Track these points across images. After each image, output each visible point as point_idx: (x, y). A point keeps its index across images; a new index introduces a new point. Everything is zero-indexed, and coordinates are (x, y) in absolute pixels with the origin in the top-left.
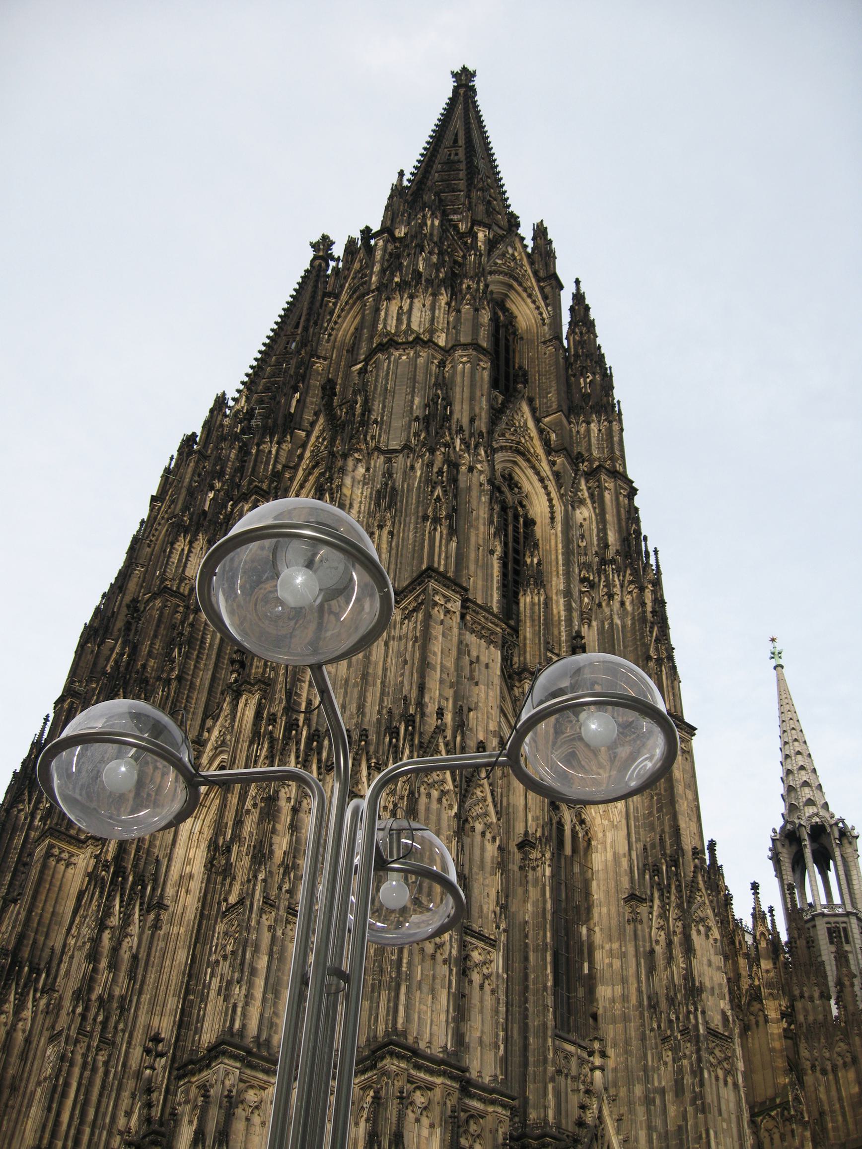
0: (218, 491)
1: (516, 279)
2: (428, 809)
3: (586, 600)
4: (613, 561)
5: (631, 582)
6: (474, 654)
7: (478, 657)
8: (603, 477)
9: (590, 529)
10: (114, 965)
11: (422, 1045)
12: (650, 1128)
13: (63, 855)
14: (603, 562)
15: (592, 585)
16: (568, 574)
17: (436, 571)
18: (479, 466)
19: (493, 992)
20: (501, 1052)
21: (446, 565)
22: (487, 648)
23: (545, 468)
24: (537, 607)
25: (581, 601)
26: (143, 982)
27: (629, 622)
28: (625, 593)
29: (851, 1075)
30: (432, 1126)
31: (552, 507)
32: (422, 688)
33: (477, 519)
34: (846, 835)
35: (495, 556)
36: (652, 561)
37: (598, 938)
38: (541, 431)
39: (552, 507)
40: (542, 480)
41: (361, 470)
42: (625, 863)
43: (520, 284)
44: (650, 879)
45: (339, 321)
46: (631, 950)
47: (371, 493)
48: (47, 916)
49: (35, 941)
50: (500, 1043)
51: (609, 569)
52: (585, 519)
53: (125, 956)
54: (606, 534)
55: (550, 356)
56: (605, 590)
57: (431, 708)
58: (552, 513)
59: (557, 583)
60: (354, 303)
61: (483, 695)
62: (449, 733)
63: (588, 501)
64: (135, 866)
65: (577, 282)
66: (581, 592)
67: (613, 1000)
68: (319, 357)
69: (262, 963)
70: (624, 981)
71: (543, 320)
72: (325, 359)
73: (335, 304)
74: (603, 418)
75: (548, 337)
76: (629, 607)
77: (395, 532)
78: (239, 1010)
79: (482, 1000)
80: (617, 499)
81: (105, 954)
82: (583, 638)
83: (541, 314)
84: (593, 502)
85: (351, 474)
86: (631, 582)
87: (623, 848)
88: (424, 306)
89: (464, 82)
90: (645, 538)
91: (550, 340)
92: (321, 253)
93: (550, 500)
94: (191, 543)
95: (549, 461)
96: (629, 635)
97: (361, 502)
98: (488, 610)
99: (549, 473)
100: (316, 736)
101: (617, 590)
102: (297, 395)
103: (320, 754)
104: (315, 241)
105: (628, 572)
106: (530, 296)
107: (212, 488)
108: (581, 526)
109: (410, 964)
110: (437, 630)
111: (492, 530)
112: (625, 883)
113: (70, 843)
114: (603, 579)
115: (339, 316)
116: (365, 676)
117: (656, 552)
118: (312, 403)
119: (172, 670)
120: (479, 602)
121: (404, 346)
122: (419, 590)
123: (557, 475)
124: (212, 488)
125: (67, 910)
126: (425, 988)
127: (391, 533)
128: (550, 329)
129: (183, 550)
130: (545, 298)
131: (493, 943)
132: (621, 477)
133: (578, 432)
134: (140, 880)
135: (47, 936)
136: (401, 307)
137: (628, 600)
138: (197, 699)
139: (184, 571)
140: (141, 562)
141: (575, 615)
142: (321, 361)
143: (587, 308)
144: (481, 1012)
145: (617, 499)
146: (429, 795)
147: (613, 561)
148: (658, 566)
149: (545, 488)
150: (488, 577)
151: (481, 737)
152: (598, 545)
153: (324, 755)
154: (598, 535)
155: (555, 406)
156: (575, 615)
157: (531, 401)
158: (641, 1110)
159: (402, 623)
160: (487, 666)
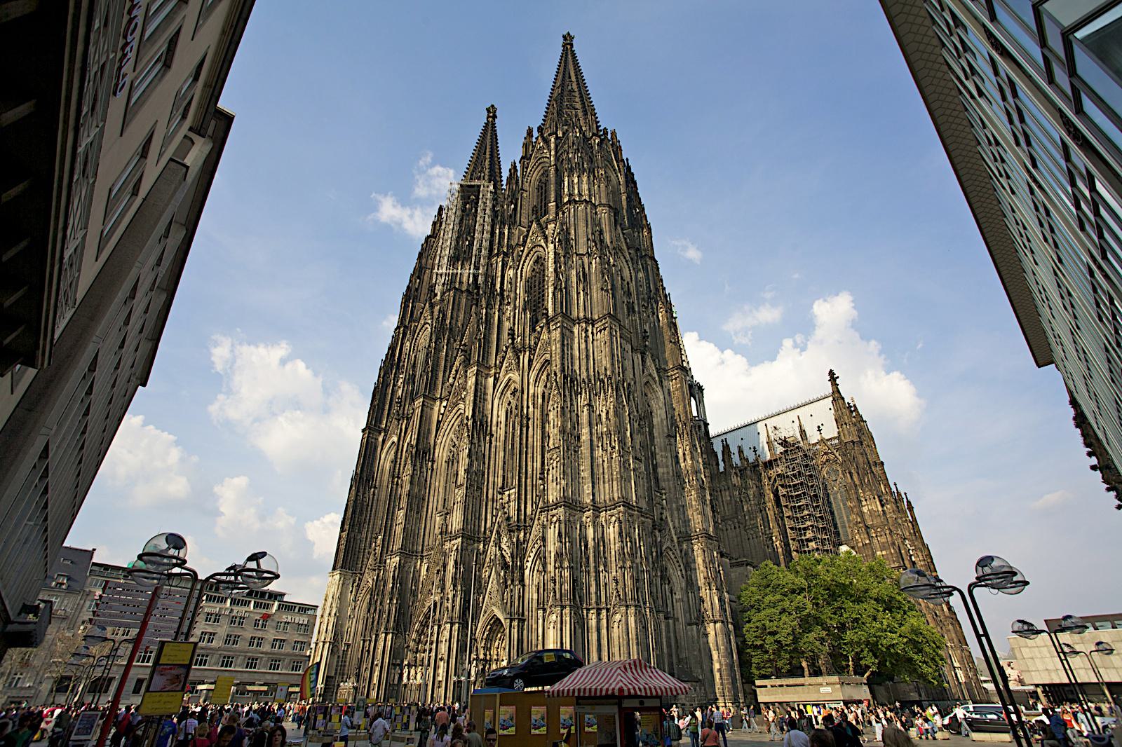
12: (679, 519)
14: (649, 298)
15: (646, 308)
16: (638, 304)
29: (727, 493)
34: (701, 389)
37: (657, 451)
40: (627, 261)
46: (669, 455)
67: (663, 473)
70: (667, 467)
131: (641, 461)
143: (633, 174)
158: (675, 512)
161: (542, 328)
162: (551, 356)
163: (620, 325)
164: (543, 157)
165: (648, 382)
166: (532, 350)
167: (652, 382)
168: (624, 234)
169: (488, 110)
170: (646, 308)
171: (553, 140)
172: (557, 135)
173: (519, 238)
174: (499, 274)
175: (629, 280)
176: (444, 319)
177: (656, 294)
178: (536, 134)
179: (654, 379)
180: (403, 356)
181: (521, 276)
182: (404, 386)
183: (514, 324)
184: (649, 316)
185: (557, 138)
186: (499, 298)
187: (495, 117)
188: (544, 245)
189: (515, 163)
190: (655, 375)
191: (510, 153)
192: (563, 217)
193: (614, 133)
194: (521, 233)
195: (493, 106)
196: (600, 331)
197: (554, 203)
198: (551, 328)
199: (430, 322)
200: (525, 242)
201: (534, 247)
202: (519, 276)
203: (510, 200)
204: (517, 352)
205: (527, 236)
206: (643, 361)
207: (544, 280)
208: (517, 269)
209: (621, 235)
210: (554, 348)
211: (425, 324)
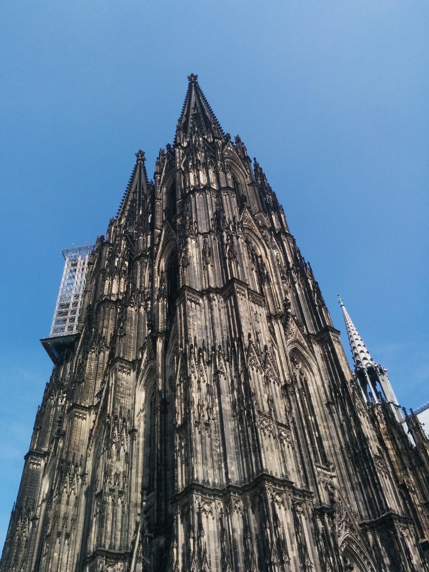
0: (120, 258)
2: (253, 375)
3: (285, 285)
6: (255, 310)
7: (256, 312)
10: (118, 459)
11: (274, 475)
13: (81, 415)
14: (289, 269)
17: (235, 279)
18: (240, 236)
19: (293, 448)
20: (302, 473)
21: (238, 276)
22: (259, 308)
25: (283, 286)
26: (132, 464)
30: (285, 509)
32: (240, 326)
33: (244, 257)
35: (254, 271)
38: (255, 220)
40: (259, 239)
41: (194, 242)
42: (322, 389)
43: (235, 162)
44: (335, 393)
47: (200, 251)
48: (77, 442)
49: (74, 454)
50: (301, 470)
53: (122, 453)
55: (252, 190)
57: (245, 334)
59: (274, 279)
60: (169, 176)
61: (261, 327)
62: (254, 343)
64: (121, 414)
65: (255, 159)
66: (283, 282)
68: (158, 199)
69: (199, 448)
72: (161, 200)
73: (160, 177)
75: (249, 182)
78: (195, 469)
79: (289, 453)
80: (289, 244)
81: (115, 454)
82: (288, 300)
85: (190, 244)
87: (320, 383)
88: (204, 173)
90: (303, 258)
91: (251, 183)
93: (264, 247)
94: (112, 280)
97: (196, 255)
98: (256, 292)
100: (200, 351)
103: (203, 358)
106: (240, 166)
107: (117, 256)
109: (262, 440)
110: (240, 303)
112: (324, 397)
113: (83, 410)
116: (213, 324)
117: (309, 263)
118: (159, 218)
119: (122, 332)
120: (252, 289)
122: (230, 287)
123: (264, 237)
124: (117, 256)
125: (85, 438)
126: (270, 450)
127: (212, 266)
129: (109, 283)
130: (245, 166)
131: (288, 427)
134: (124, 421)
135: (78, 450)
136: (195, 175)
139: (111, 291)
140: (88, 290)
141: (283, 291)
142: (159, 200)
144: (290, 457)
145: (289, 244)
146: (253, 369)
147: (293, 269)
150: (253, 280)
151: (265, 344)
156: (283, 291)
157: (249, 208)
160: (260, 315)
163: (248, 289)
171: (178, 150)
175: (264, 255)
179: (302, 345)
190: (304, 341)
201: (168, 242)
206: (285, 326)
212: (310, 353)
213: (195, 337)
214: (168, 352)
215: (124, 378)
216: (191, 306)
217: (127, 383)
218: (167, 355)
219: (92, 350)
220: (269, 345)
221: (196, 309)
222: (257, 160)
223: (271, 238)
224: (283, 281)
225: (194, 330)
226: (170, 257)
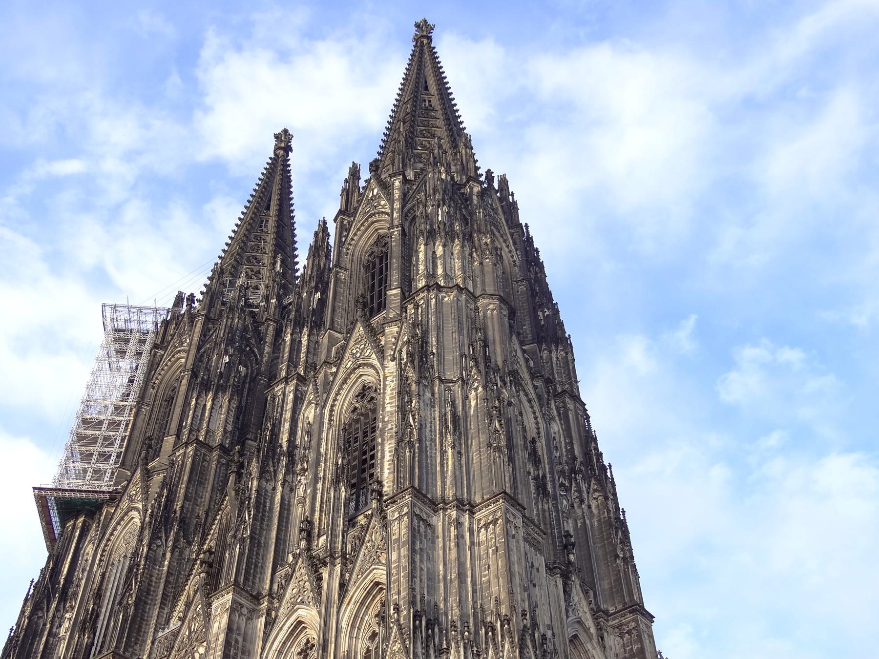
1: (497, 229)
3: (565, 502)
4: (581, 471)
5: (595, 491)
8: (567, 400)
9: (560, 442)
14: (573, 471)
16: (553, 481)
23: (530, 388)
24: (547, 514)
27: (596, 523)
28: (591, 499)
31: (537, 423)
36: (609, 474)
39: (537, 423)
40: (530, 401)
45: (355, 238)
51: (579, 477)
52: (555, 433)
54: (573, 448)
56: (576, 494)
58: (538, 429)
63: (557, 418)
68: (341, 268)
71: (514, 261)
72: (346, 270)
74: (560, 348)
76: (595, 511)
77: (463, 451)
83: (512, 257)
84: (560, 420)
86: (595, 491)
89: (425, 33)
91: (522, 281)
92: (283, 145)
93: (536, 418)
95: (534, 385)
96: (597, 533)
99: (534, 396)
101: (585, 495)
102: (318, 295)
104: (277, 132)
105: (593, 481)
106: (505, 241)
108: (554, 438)
111: (527, 456)
114: (574, 485)
115: (355, 234)
117: (610, 466)
121: (445, 290)
123: (540, 398)
128: (520, 271)
132: (576, 398)
133: (541, 357)
136: (434, 252)
137: (594, 504)
138: (263, 555)
148: (612, 478)
149: (532, 407)
150: (529, 492)
152: (567, 456)
153: (437, 640)
154: (566, 447)
155: (530, 337)
159: (479, 532)
160: (538, 570)
161: (369, 518)
162: (389, 574)
164: (379, 213)
165: (575, 637)
166: (348, 561)
167: (583, 637)
168: (524, 351)
169: (277, 137)
170: (568, 490)
171: (397, 183)
172: (404, 177)
173: (329, 351)
174: (288, 415)
176: (170, 500)
177: (588, 467)
178: (365, 174)
179: (587, 630)
180: (78, 573)
181: (330, 420)
182: (71, 637)
183: (313, 511)
184: (572, 506)
185: (405, 181)
186: (284, 460)
187: (288, 149)
188: (376, 363)
189: (325, 223)
191: (315, 207)
192: (416, 313)
193: (504, 182)
194: (332, 341)
195: (286, 131)
196: (486, 526)
197: (398, 291)
198: (389, 518)
199: (140, 506)
200: (340, 357)
202: (326, 421)
203: (313, 284)
204: (315, 565)
205: (343, 349)
207: (374, 430)
208: (324, 407)
209: (519, 353)
210: (394, 556)
211: (130, 509)
212: (598, 649)
213: (423, 597)
214: (346, 600)
215: (239, 629)
216: (419, 530)
217: (244, 640)
218: (344, 606)
219: (159, 542)
220: (549, 635)
221: (426, 538)
222: (529, 229)
223: (548, 399)
224: (562, 493)
225: (421, 581)
226: (357, 396)
